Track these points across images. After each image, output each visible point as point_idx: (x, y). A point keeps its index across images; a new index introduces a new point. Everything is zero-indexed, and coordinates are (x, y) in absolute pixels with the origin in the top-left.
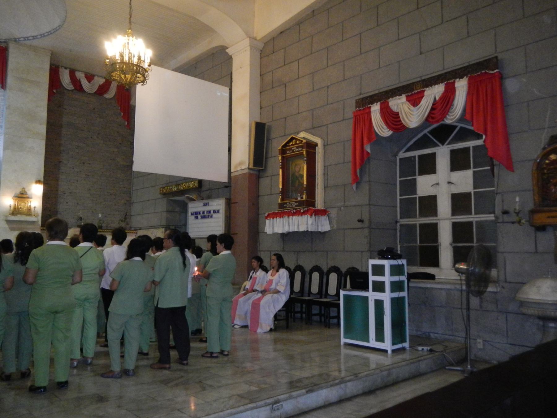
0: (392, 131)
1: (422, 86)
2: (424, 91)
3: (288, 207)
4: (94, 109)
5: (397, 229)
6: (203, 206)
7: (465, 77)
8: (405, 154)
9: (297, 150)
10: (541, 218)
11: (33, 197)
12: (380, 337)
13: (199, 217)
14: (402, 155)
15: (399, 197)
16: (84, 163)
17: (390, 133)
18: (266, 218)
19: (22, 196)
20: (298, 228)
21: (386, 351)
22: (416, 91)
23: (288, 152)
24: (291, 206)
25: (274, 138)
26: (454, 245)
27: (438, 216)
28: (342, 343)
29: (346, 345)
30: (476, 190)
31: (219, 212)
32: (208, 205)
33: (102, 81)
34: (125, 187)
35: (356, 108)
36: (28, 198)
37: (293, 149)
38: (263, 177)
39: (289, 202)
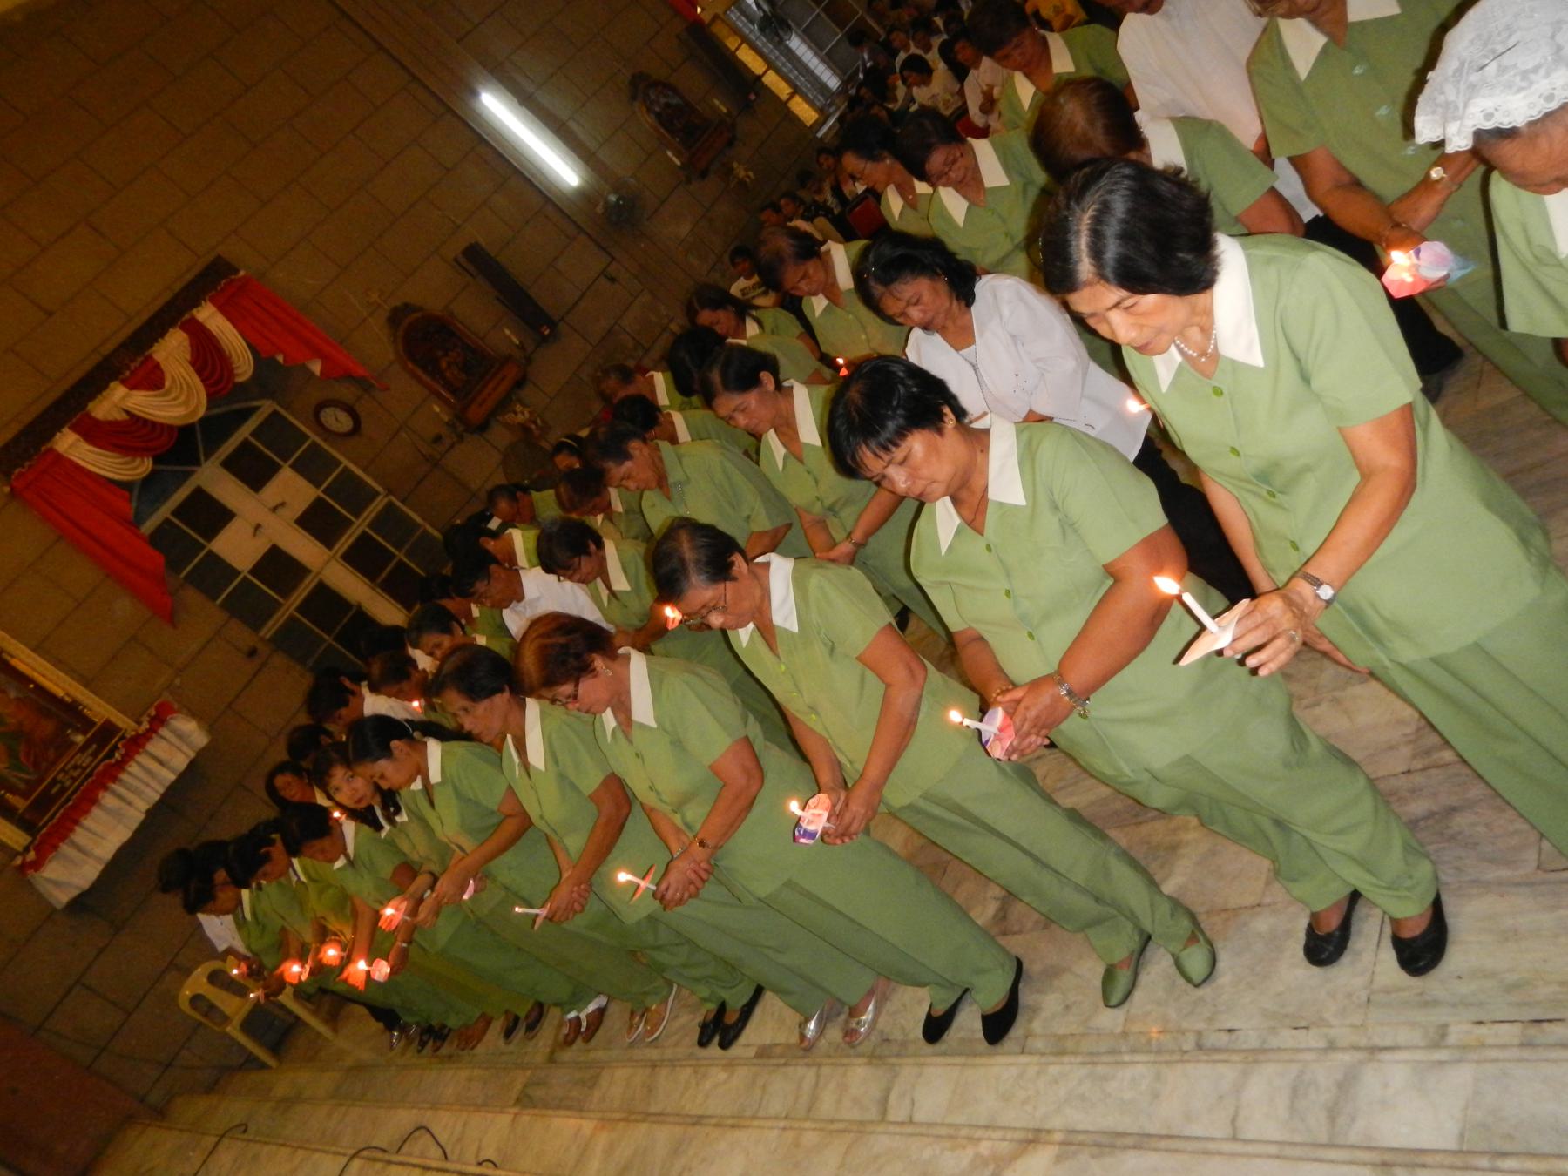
0: (148, 457)
2: (150, 357)
3: (68, 783)
10: (476, 413)
20: (172, 770)
24: (78, 771)
39: (63, 770)
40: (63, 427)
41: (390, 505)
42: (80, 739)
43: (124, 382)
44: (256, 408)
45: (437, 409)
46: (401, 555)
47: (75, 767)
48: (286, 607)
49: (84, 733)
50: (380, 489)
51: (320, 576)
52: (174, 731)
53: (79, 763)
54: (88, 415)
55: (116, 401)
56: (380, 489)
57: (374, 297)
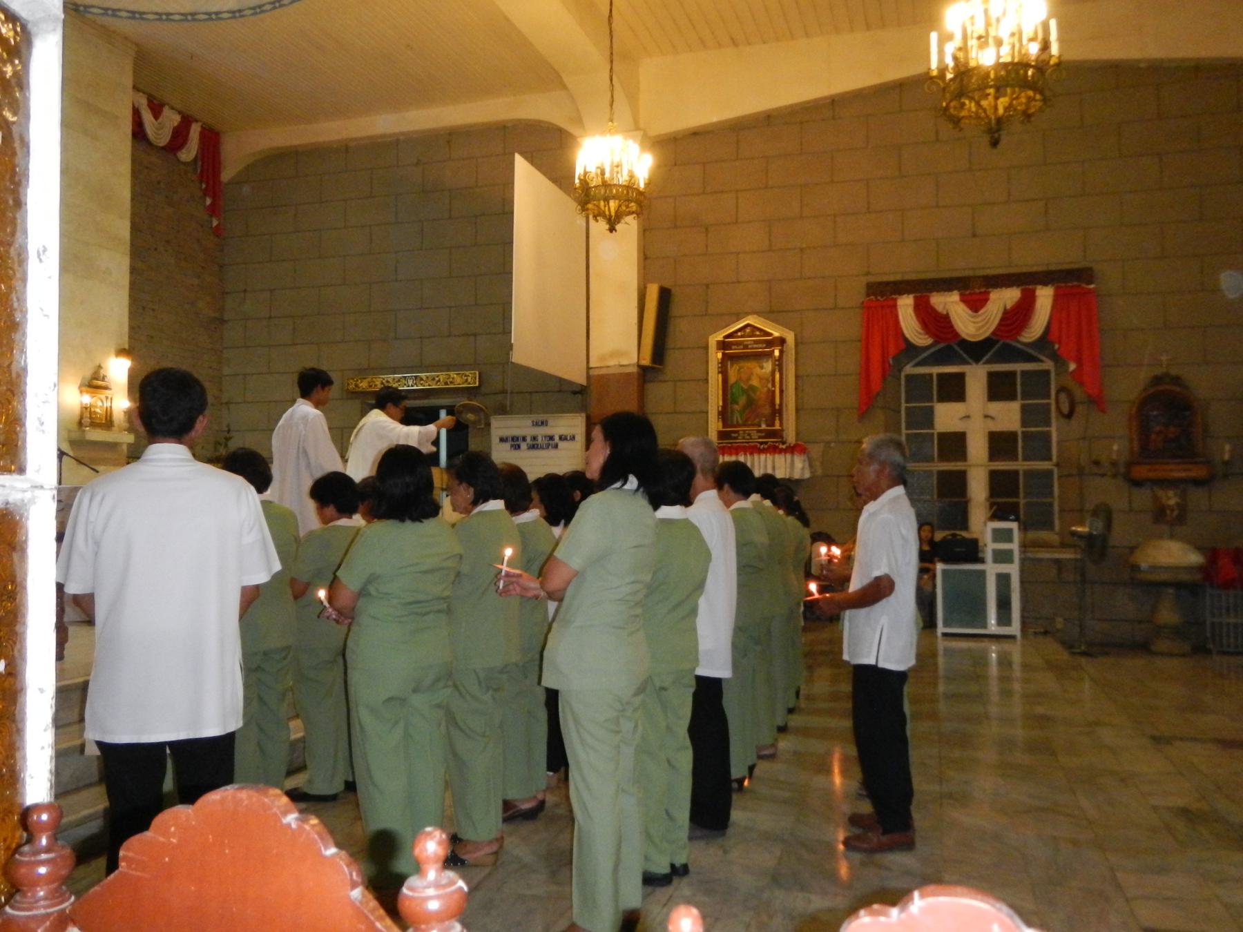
2: (988, 293)
3: (740, 438)
4: (159, 183)
6: (533, 425)
8: (912, 369)
9: (755, 346)
10: (1141, 472)
11: (112, 386)
12: (1004, 618)
13: (524, 446)
14: (909, 369)
16: (144, 308)
19: (95, 383)
21: (1012, 637)
23: (733, 347)
24: (748, 437)
26: (992, 500)
29: (945, 635)
31: (573, 438)
32: (547, 425)
33: (176, 119)
34: (211, 368)
35: (868, 295)
36: (106, 388)
37: (745, 343)
38: (652, 381)
44: (1041, 361)
46: (1022, 501)
47: (749, 435)
48: (935, 464)
49: (768, 426)
52: (793, 461)
54: (928, 299)
55: (949, 303)
57: (1164, 358)
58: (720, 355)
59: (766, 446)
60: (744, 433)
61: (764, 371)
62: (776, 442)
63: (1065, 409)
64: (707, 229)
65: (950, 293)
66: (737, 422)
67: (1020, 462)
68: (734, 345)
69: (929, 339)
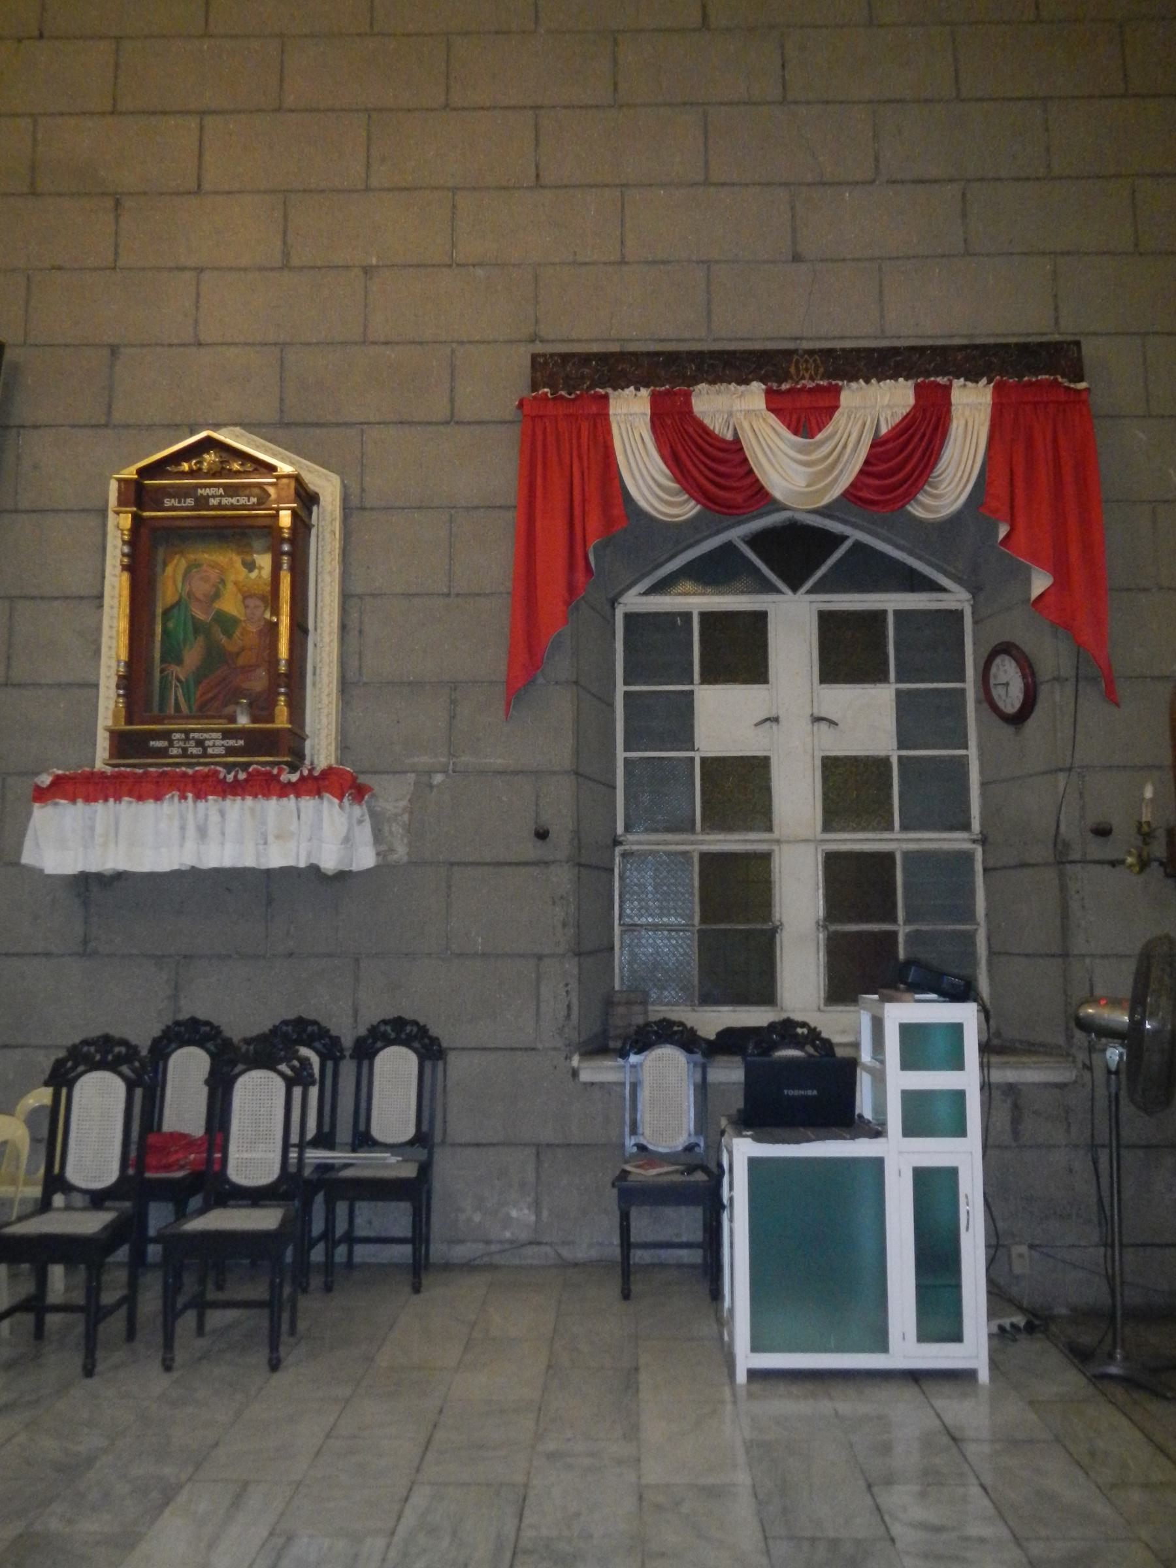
0: (698, 502)
1: (821, 370)
2: (837, 390)
3: (174, 751)
5: (612, 870)
7: (984, 380)
8: (645, 599)
14: (635, 601)
15: (621, 755)
17: (691, 510)
18: (41, 795)
21: (969, 1375)
22: (811, 385)
23: (168, 503)
25: (36, 427)
26: (833, 928)
27: (776, 828)
28: (741, 1377)
30: (904, 753)
35: (535, 387)
39: (187, 732)
40: (646, 386)
41: (966, 858)
42: (243, 721)
43: (771, 396)
44: (943, 589)
45: (1148, 793)
46: (902, 930)
47: (200, 743)
49: (254, 720)
50: (976, 825)
51: (775, 848)
53: (207, 743)
54: (688, 396)
56: (976, 825)
58: (126, 521)
59: (242, 776)
60: (187, 739)
61: (254, 575)
62: (273, 764)
63: (1011, 698)
64: (118, 204)
65: (743, 388)
66: (177, 708)
67: (897, 834)
68: (171, 496)
69: (693, 503)
